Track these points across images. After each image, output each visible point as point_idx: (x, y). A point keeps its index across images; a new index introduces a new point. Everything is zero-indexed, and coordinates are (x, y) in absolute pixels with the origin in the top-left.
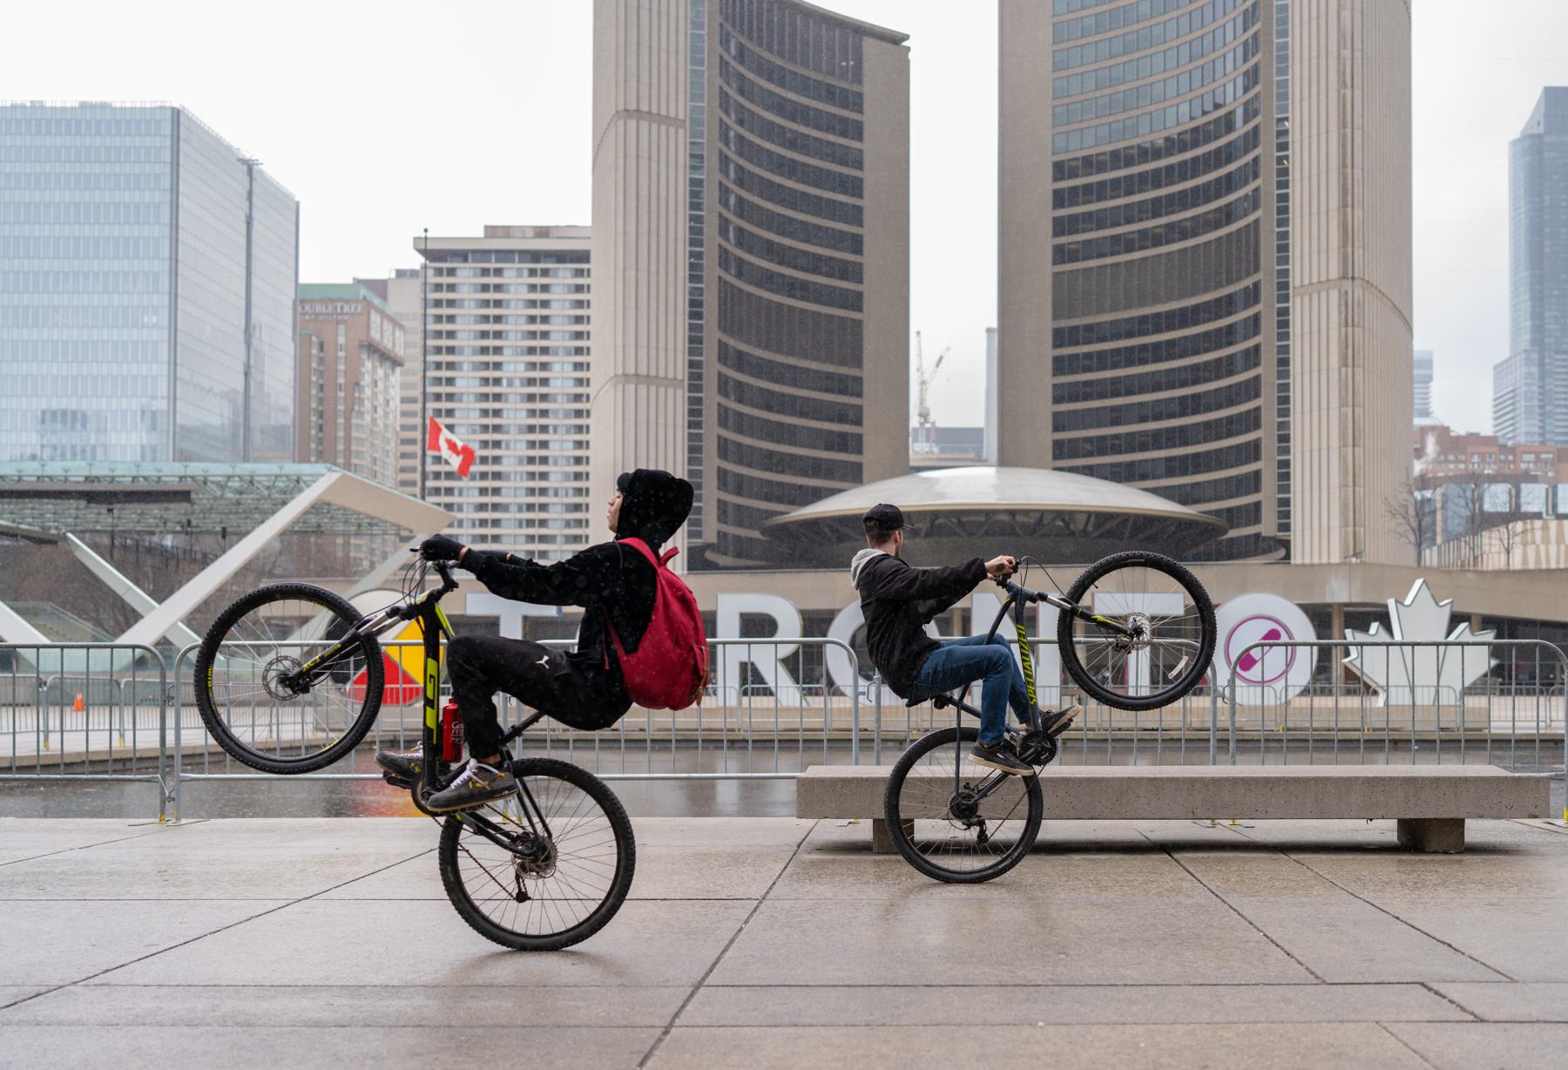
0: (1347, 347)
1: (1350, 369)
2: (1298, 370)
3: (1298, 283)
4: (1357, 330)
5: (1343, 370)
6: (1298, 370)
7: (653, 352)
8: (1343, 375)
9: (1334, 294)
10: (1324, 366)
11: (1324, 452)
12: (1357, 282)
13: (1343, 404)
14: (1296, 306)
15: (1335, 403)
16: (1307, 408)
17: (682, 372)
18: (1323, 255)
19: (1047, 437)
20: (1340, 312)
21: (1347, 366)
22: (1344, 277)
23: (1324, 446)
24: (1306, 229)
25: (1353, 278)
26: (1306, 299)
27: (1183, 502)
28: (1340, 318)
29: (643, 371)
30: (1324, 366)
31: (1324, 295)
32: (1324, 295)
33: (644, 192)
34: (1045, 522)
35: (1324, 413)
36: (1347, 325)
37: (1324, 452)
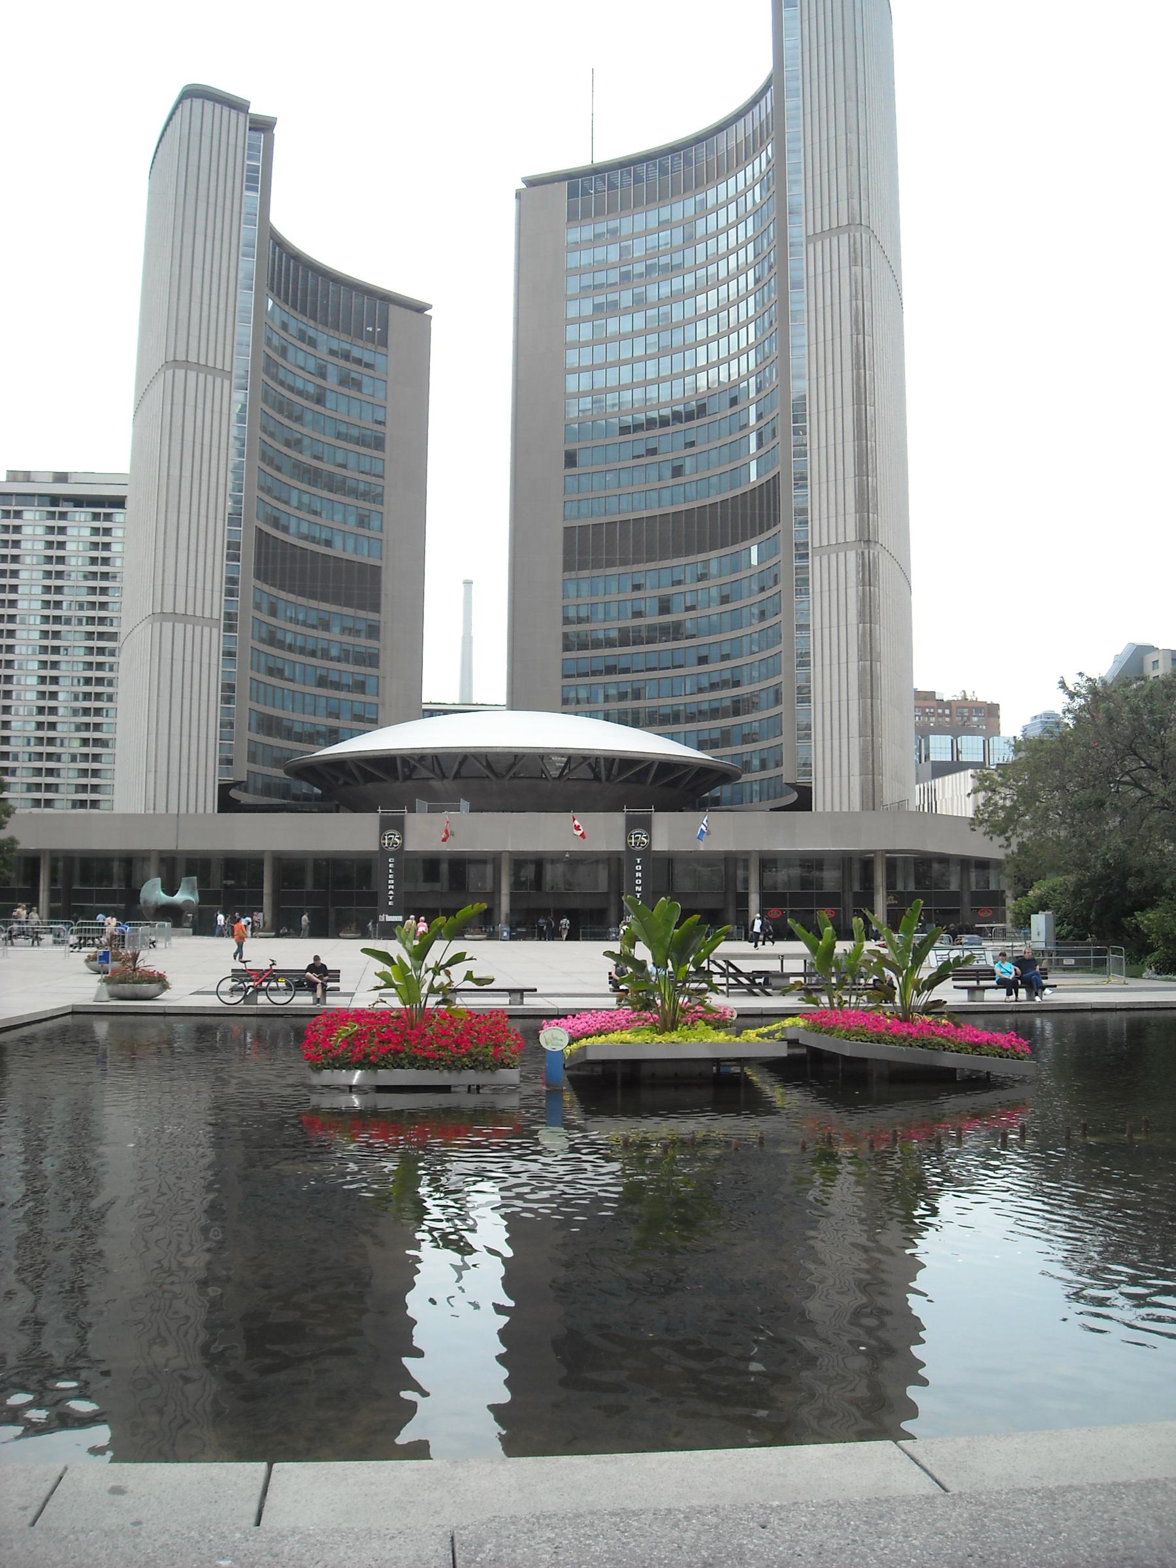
0: (864, 606)
2: (818, 626)
3: (817, 545)
5: (861, 625)
6: (818, 626)
7: (191, 591)
9: (852, 556)
10: (843, 623)
11: (844, 704)
12: (872, 545)
14: (815, 565)
16: (827, 662)
17: (218, 613)
18: (841, 519)
19: (557, 682)
20: (858, 573)
23: (844, 697)
24: (824, 495)
25: (869, 541)
26: (825, 558)
27: (700, 747)
28: (857, 578)
29: (180, 610)
30: (843, 623)
31: (841, 555)
32: (841, 555)
33: (189, 438)
34: (572, 766)
35: (844, 666)
36: (863, 585)
37: (844, 704)
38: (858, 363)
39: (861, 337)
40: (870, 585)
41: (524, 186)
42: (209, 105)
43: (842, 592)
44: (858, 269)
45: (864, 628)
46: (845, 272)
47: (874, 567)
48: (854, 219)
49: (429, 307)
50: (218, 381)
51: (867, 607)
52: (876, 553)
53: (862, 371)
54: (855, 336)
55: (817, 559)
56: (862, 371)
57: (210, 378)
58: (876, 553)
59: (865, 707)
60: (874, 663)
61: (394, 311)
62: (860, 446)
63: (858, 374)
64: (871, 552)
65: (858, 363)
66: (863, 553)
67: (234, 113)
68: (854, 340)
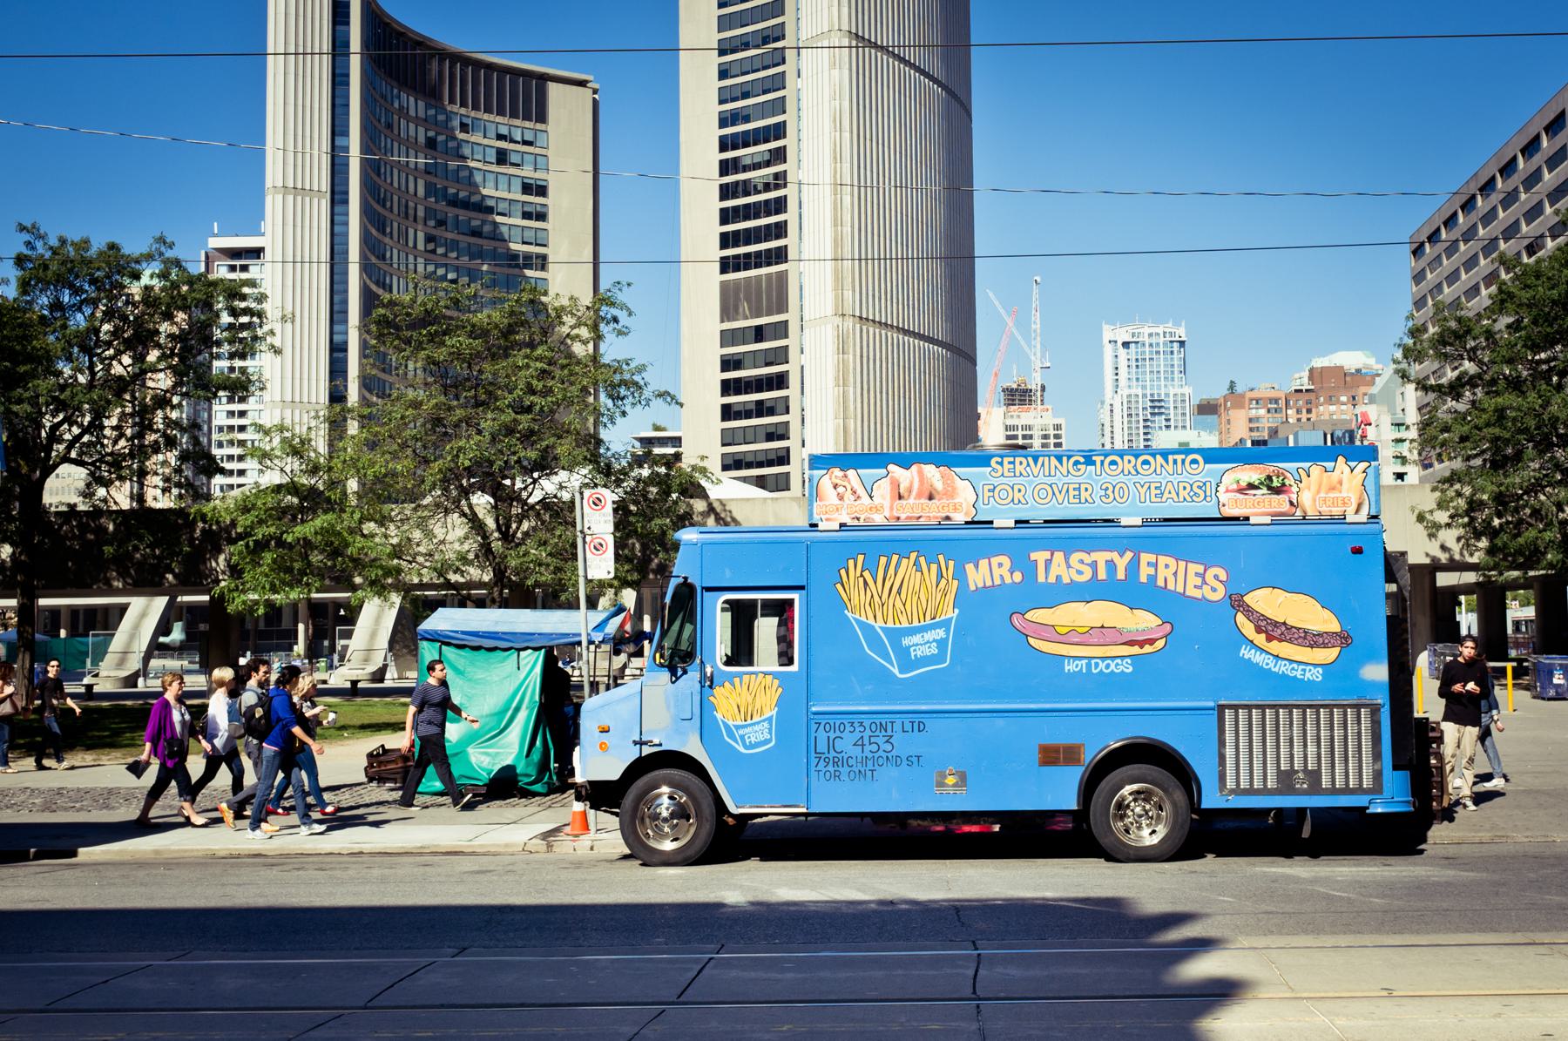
5: (836, 389)
8: (836, 393)
9: (829, 327)
12: (847, 317)
30: (824, 386)
39: (838, 134)
43: (823, 359)
44: (836, 72)
46: (826, 74)
48: (833, 25)
54: (833, 134)
56: (839, 165)
61: (553, 89)
62: (836, 232)
63: (835, 168)
65: (835, 158)
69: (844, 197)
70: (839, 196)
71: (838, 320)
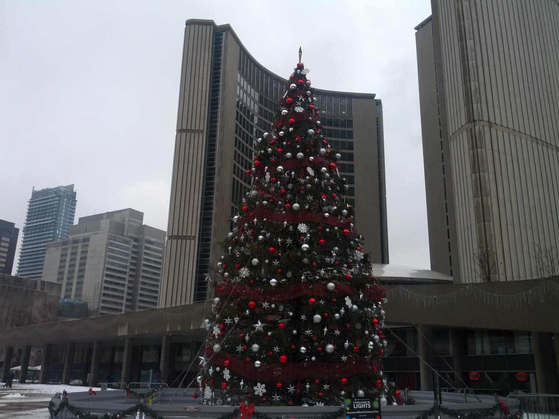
0: (474, 162)
1: (478, 174)
4: (479, 150)
5: (474, 174)
9: (465, 133)
11: (469, 228)
13: (475, 196)
15: (471, 197)
20: (469, 142)
21: (475, 173)
22: (469, 122)
25: (474, 121)
26: (455, 140)
36: (473, 149)
38: (459, 19)
40: (477, 148)
41: (417, 31)
42: (193, 26)
45: (476, 177)
47: (480, 135)
49: (374, 95)
50: (197, 135)
51: (476, 162)
52: (481, 128)
53: (462, 22)
54: (456, 5)
55: (452, 142)
56: (462, 22)
57: (193, 134)
58: (481, 128)
59: (480, 229)
60: (484, 198)
62: (464, 66)
64: (477, 128)
65: (459, 19)
66: (471, 129)
67: (205, 27)
68: (456, 7)
69: (468, 42)
70: (464, 42)
71: (470, 125)
